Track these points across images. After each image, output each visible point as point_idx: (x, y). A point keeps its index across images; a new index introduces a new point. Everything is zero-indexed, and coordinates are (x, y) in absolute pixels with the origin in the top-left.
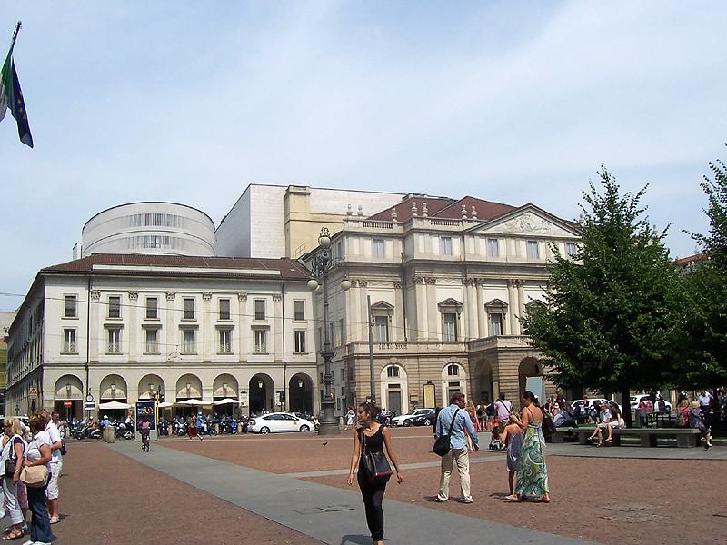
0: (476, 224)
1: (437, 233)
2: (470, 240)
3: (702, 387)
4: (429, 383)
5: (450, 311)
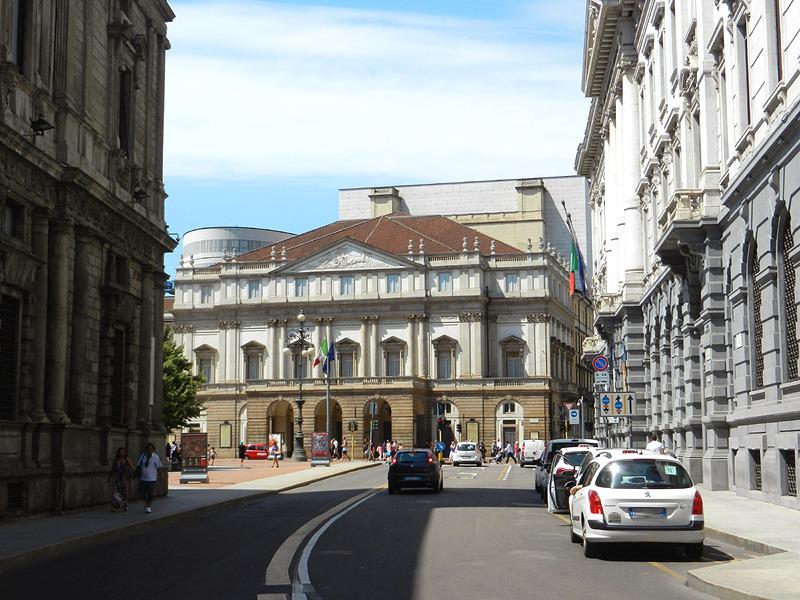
4: (226, 423)
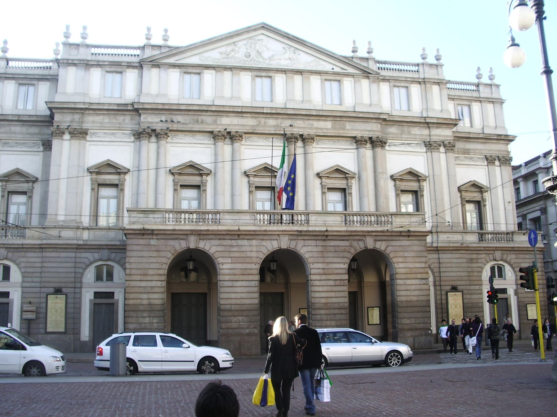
0: (168, 49)
1: (99, 65)
2: (152, 75)
4: (58, 291)
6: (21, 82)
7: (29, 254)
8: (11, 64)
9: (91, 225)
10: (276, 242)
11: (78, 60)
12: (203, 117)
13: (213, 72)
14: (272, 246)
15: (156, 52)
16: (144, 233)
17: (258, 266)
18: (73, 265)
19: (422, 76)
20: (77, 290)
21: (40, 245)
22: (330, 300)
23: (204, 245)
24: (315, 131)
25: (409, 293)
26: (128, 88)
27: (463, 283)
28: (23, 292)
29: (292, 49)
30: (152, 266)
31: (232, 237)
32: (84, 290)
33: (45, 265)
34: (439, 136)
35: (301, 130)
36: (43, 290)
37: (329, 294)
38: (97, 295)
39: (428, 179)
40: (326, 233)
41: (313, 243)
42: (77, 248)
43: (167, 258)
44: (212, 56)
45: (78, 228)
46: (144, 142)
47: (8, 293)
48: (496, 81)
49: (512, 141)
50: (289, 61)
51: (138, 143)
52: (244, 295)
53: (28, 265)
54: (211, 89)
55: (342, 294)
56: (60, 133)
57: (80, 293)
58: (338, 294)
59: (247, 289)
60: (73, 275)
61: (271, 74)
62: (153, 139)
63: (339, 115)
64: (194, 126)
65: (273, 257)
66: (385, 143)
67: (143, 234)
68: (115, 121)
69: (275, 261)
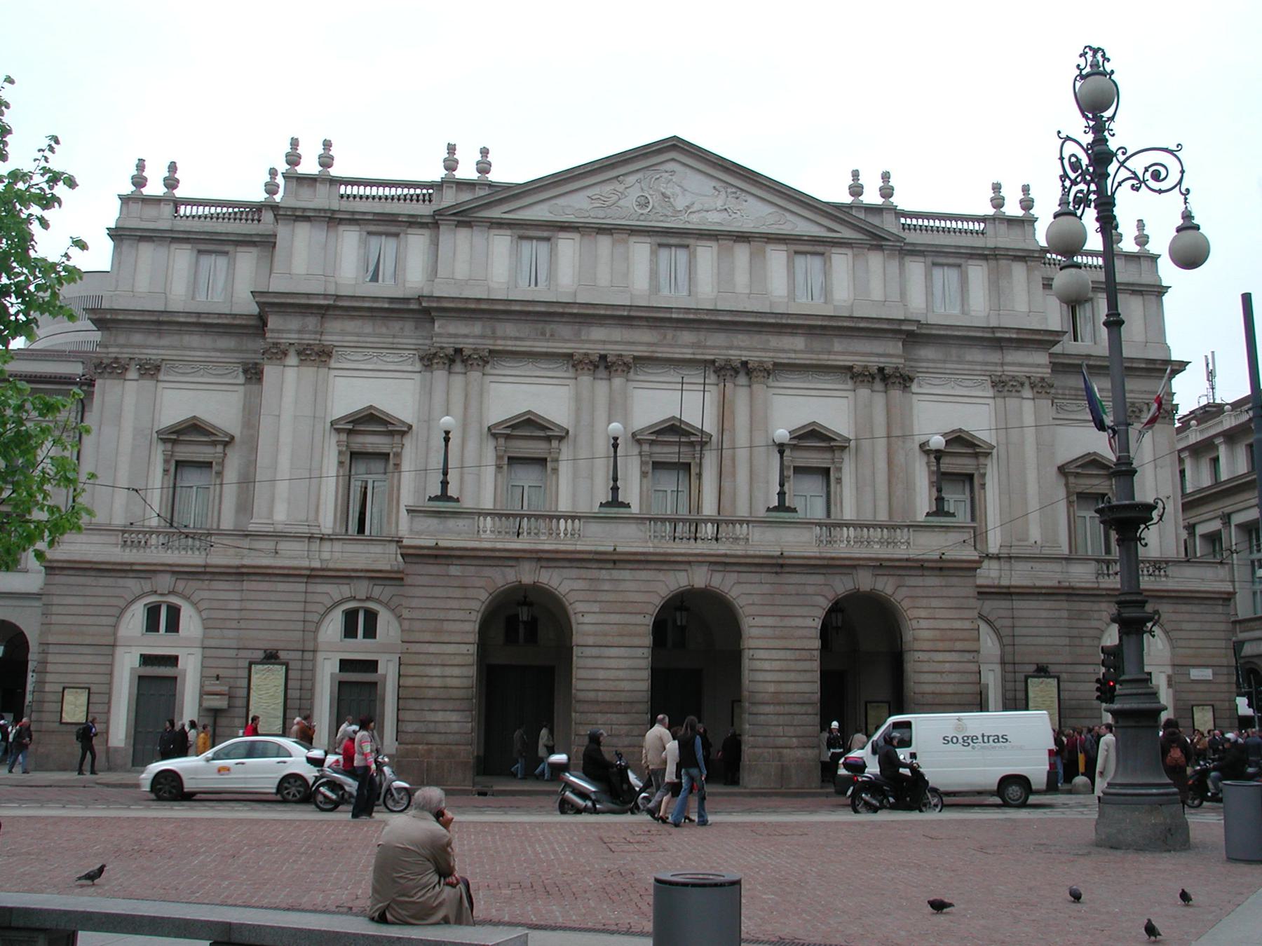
0: (487, 191)
1: (353, 220)
3: (382, 771)
4: (271, 657)
5: (368, 440)
6: (202, 247)
7: (215, 585)
8: (182, 210)
9: (338, 531)
10: (684, 574)
11: (315, 210)
12: (553, 326)
13: (577, 236)
14: (677, 581)
15: (466, 196)
16: (438, 556)
17: (650, 620)
18: (300, 607)
19: (991, 244)
20: (308, 656)
21: (238, 567)
22: (785, 688)
23: (551, 579)
24: (771, 354)
25: (938, 678)
26: (413, 267)
27: (1060, 659)
28: (204, 657)
29: (729, 190)
30: (451, 615)
31: (601, 565)
32: (320, 656)
33: (248, 605)
34: (1021, 365)
35: (744, 353)
36: (243, 653)
37: (782, 677)
38: (345, 665)
39: (995, 451)
40: (781, 561)
41: (755, 578)
42: (309, 576)
43: (479, 600)
44: (576, 206)
45: (311, 538)
46: (440, 375)
47: (176, 658)
48: (1152, 248)
49: (1178, 372)
50: (725, 215)
51: (428, 374)
52: (621, 674)
53: (215, 604)
54: (568, 272)
55: (808, 676)
56: (278, 353)
57: (314, 660)
58: (800, 677)
59: (628, 663)
60: (300, 626)
61: (691, 242)
62: (458, 367)
63: (820, 323)
64: (537, 344)
65: (682, 602)
66: (911, 380)
67: (436, 556)
68: (384, 330)
69: (687, 609)
